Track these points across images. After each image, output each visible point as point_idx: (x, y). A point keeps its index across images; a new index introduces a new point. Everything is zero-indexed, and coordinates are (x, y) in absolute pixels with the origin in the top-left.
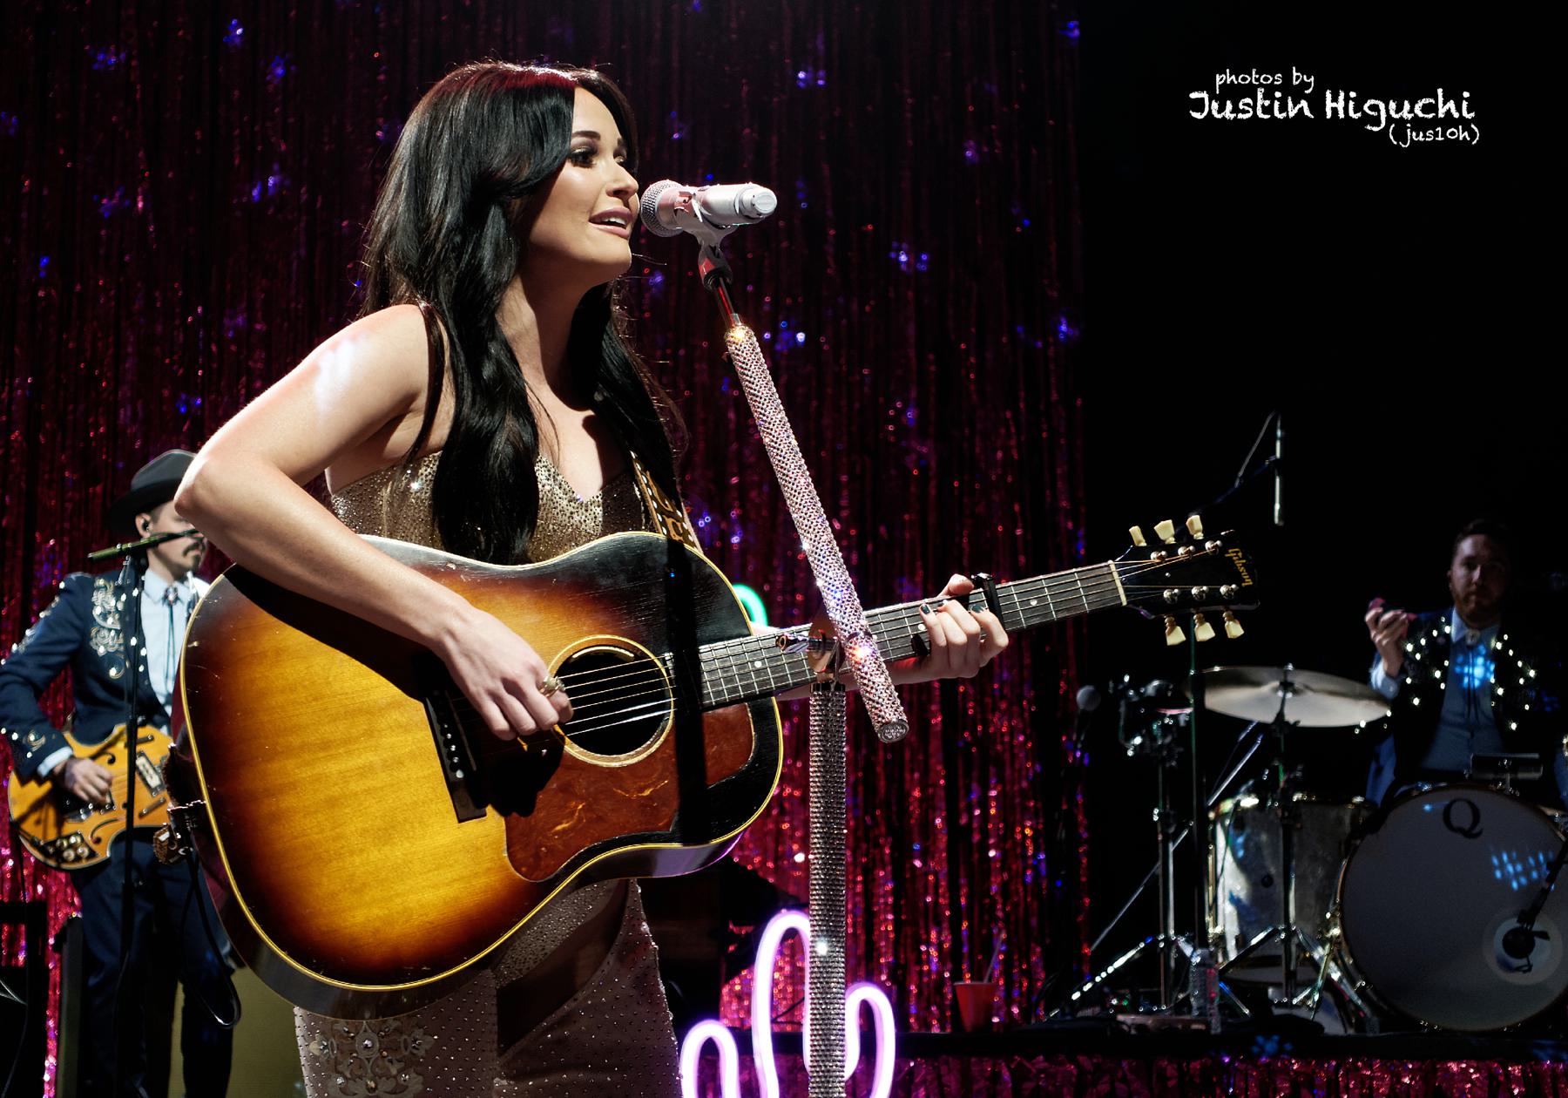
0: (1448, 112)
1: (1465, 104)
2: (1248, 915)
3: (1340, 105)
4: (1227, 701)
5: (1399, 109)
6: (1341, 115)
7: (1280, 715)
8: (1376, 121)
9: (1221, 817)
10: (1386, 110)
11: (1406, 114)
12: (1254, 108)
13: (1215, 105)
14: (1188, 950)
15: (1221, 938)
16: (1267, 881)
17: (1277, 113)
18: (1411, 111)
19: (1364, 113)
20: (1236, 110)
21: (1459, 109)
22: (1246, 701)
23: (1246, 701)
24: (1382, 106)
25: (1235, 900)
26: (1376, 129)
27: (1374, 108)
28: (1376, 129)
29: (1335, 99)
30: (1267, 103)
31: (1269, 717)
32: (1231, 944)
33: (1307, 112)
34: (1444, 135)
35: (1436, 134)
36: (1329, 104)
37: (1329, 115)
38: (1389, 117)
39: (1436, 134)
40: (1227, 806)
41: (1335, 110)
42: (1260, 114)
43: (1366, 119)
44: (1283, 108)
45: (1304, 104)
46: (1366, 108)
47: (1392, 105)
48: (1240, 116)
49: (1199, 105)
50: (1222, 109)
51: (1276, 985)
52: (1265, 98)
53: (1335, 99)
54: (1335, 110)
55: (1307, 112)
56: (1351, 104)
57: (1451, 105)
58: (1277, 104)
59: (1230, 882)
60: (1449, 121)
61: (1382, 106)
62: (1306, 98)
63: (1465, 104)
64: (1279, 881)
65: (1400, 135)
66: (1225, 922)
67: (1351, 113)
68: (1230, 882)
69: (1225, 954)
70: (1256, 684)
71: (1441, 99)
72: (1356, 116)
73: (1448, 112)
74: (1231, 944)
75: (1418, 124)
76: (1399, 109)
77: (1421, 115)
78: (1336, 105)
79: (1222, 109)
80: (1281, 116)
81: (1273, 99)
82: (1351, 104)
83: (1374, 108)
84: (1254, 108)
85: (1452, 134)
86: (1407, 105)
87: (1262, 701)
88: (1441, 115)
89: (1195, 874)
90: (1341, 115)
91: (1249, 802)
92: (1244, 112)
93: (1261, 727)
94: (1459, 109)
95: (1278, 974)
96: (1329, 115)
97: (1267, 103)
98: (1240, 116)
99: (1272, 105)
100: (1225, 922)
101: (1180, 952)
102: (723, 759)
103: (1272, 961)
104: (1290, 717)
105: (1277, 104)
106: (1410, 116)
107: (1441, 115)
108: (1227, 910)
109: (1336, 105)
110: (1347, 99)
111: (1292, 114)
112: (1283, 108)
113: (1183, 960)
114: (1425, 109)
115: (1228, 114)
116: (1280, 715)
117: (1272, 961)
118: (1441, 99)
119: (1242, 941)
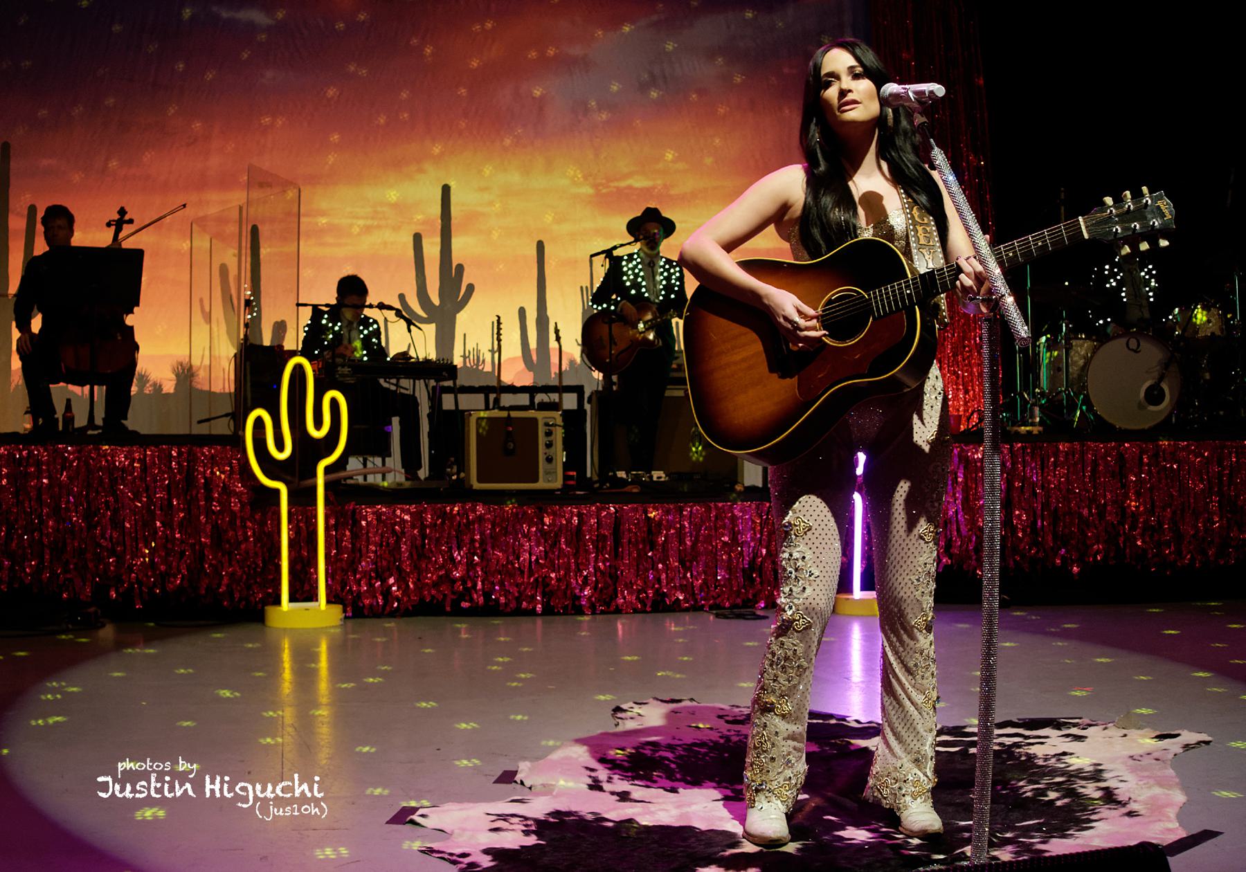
1: (316, 786)
6: (218, 795)
12: (149, 789)
13: (117, 787)
19: (236, 793)
20: (134, 791)
21: (311, 790)
27: (244, 789)
33: (190, 793)
48: (138, 795)
49: (105, 787)
50: (123, 790)
55: (190, 793)
63: (316, 786)
71: (297, 782)
79: (123, 790)
92: (140, 792)
94: (311, 790)
98: (138, 795)
111: (178, 794)
115: (128, 794)
118: (297, 782)
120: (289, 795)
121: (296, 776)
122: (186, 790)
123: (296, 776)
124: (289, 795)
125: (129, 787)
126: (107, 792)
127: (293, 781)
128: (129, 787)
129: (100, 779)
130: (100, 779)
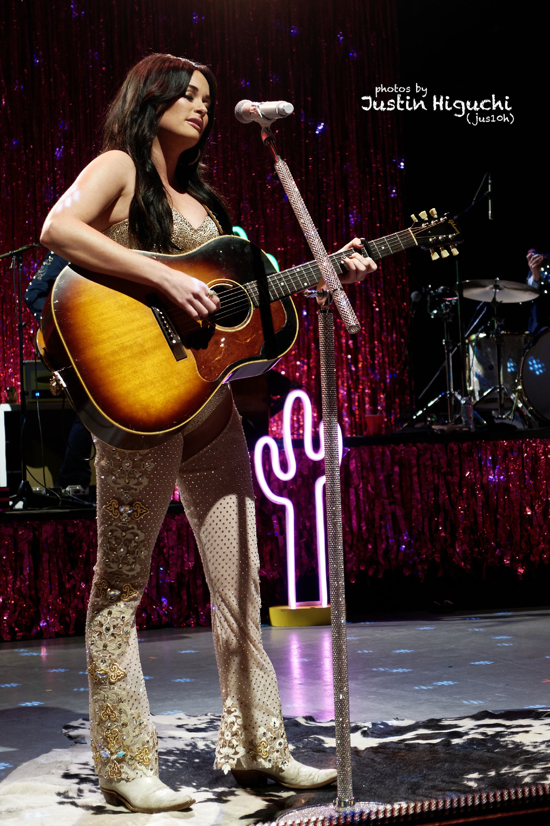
0: (498, 107)
2: (484, 382)
3: (441, 103)
4: (472, 294)
5: (472, 105)
6: (442, 109)
7: (494, 299)
8: (460, 112)
9: (470, 342)
10: (465, 106)
11: (475, 108)
13: (375, 103)
14: (459, 397)
15: (473, 392)
16: (491, 368)
17: (407, 108)
18: (478, 106)
19: (453, 107)
20: (386, 106)
22: (479, 294)
23: (479, 294)
24: (463, 104)
25: (478, 376)
26: (459, 116)
28: (459, 116)
29: (438, 100)
30: (402, 102)
31: (490, 300)
32: (477, 394)
33: (423, 107)
34: (495, 119)
35: (491, 119)
36: (435, 103)
37: (435, 109)
38: (467, 110)
39: (491, 119)
40: (473, 337)
41: (438, 106)
42: (399, 108)
43: (454, 110)
44: (411, 105)
45: (422, 102)
46: (454, 105)
47: (468, 103)
48: (388, 109)
49: (366, 103)
50: (378, 106)
51: (496, 410)
52: (401, 99)
53: (438, 100)
54: (438, 106)
55: (423, 107)
56: (447, 103)
57: (499, 103)
58: (407, 103)
59: (475, 367)
60: (498, 112)
61: (463, 104)
62: (423, 99)
64: (496, 368)
65: (473, 119)
66: (474, 385)
67: (447, 108)
68: (475, 367)
69: (475, 398)
70: (484, 286)
71: (494, 100)
72: (449, 109)
73: (498, 107)
74: (477, 394)
75: (482, 113)
76: (472, 105)
77: (483, 108)
78: (438, 103)
79: (378, 106)
80: (410, 109)
81: (405, 100)
82: (447, 103)
83: (457, 105)
84: (396, 105)
85: (500, 118)
86: (476, 103)
87: (486, 293)
88: (494, 108)
89: (461, 367)
90: (442, 109)
91: (482, 335)
92: (390, 107)
93: (486, 304)
95: (497, 405)
96: (435, 109)
97: (402, 102)
98: (388, 109)
99: (405, 103)
100: (474, 385)
101: (456, 399)
102: (279, 323)
103: (493, 400)
104: (498, 300)
105: (407, 103)
106: (478, 109)
107: (494, 108)
108: (474, 379)
109: (438, 103)
110: (444, 100)
111: (415, 108)
112: (411, 105)
113: (458, 402)
114: (486, 105)
115: (382, 108)
116: (494, 299)
117: (493, 400)
118: (494, 100)
119: (481, 392)
120: (488, 109)
121: (493, 96)
122: (420, 106)
123: (493, 96)
124: (488, 109)
125: (382, 103)
126: (368, 107)
127: (492, 101)
128: (382, 103)
129: (364, 98)
130: (364, 98)
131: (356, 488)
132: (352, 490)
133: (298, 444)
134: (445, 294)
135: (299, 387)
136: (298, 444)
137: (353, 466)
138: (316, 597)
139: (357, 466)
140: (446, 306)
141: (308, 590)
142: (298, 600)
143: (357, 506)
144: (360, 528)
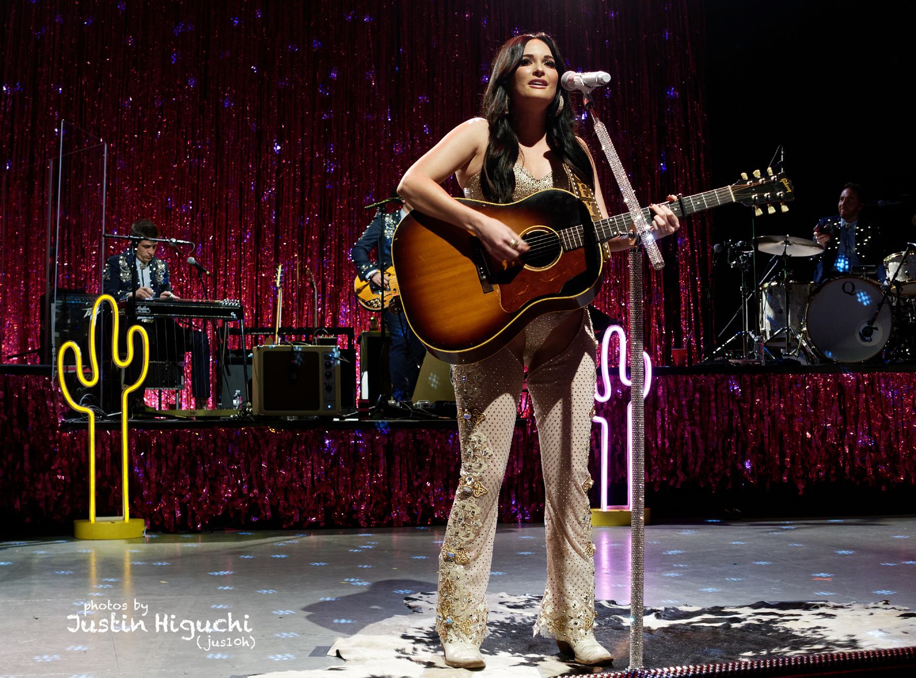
4: (765, 248)
7: (785, 253)
9: (764, 289)
14: (753, 336)
15: (765, 331)
16: (781, 311)
22: (772, 248)
23: (772, 248)
25: (769, 318)
31: (781, 254)
32: (768, 334)
40: (766, 285)
51: (784, 348)
59: (767, 312)
64: (785, 312)
66: (766, 326)
70: (776, 242)
74: (768, 334)
87: (778, 248)
91: (774, 284)
93: (778, 257)
95: (784, 344)
100: (766, 326)
101: (750, 337)
103: (782, 340)
104: (788, 254)
108: (766, 321)
113: (751, 340)
116: (785, 253)
117: (782, 340)
119: (771, 333)
131: (662, 411)
132: (658, 412)
133: (614, 372)
134: (743, 248)
135: (615, 323)
136: (614, 372)
137: (660, 392)
138: (625, 502)
139: (663, 393)
140: (743, 258)
141: (618, 495)
142: (608, 504)
143: (663, 426)
144: (663, 443)
